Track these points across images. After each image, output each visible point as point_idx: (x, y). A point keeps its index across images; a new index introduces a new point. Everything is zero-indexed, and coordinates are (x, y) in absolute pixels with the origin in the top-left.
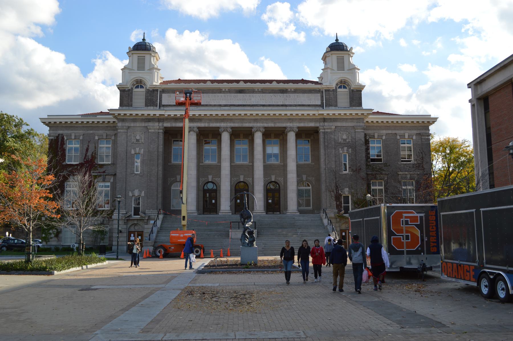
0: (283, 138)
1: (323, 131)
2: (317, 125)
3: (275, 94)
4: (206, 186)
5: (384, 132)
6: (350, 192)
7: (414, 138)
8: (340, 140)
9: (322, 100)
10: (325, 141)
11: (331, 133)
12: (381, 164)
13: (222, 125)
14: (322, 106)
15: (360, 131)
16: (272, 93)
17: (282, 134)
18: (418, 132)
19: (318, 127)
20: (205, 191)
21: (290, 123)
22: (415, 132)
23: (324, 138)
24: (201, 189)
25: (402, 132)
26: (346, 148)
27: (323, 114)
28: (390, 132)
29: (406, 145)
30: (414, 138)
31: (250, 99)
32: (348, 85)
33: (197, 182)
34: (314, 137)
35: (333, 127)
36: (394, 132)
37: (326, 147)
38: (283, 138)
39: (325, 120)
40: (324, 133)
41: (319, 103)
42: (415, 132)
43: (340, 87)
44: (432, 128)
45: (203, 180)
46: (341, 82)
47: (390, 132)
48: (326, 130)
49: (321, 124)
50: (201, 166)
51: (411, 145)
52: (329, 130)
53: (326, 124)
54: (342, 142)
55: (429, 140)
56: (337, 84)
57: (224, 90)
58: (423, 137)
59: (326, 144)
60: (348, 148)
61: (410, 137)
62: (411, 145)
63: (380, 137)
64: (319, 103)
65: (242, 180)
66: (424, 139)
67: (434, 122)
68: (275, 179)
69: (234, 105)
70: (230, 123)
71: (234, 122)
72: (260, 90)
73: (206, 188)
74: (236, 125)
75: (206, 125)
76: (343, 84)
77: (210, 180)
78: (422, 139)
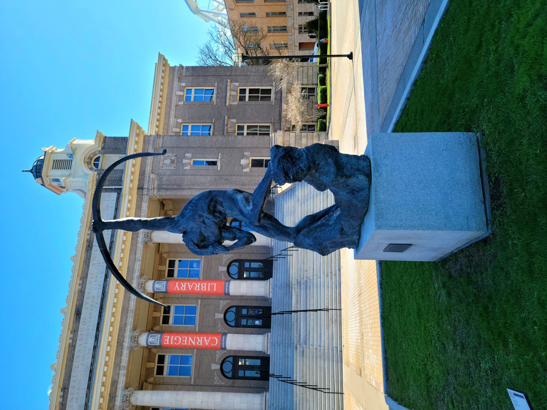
0: (166, 253)
1: (156, 190)
2: (146, 198)
3: (92, 258)
4: (227, 375)
5: (172, 120)
6: (247, 158)
7: (183, 84)
8: (172, 168)
9: (111, 190)
10: (172, 189)
11: (160, 179)
12: (214, 126)
13: (126, 344)
14: (119, 191)
15: (161, 141)
16: (89, 263)
17: (161, 254)
18: (176, 79)
19: (151, 200)
20: (235, 377)
21: (138, 237)
22: (176, 83)
23: (167, 189)
24: (230, 382)
25: (174, 98)
26: (185, 161)
27: (130, 188)
28: (173, 113)
29: (193, 95)
30: (183, 84)
31: (93, 297)
32: (95, 154)
33: (214, 391)
34: (170, 210)
35: (152, 176)
36: (173, 108)
37: (180, 187)
38: (166, 253)
39: (140, 188)
40: (159, 189)
41: (114, 195)
42: (176, 83)
43: (96, 165)
44: (172, 63)
45: (218, 379)
46: (89, 163)
47: (173, 113)
48: (156, 186)
49: (146, 193)
50: (195, 382)
51: (193, 89)
52: (156, 182)
53: (146, 186)
54: (175, 165)
55: (187, 68)
56: (91, 169)
57: (71, 341)
58: (184, 74)
59: (175, 187)
60: (185, 157)
61: (181, 89)
62: (193, 89)
63: (178, 125)
64: (114, 195)
65: (222, 316)
66: (186, 72)
67: (164, 59)
68: (224, 266)
69: (99, 324)
70: (125, 330)
71: (126, 325)
72: (81, 282)
73: (230, 375)
74: (130, 320)
75: (123, 372)
76: (94, 161)
77: (218, 367)
78: (186, 76)
